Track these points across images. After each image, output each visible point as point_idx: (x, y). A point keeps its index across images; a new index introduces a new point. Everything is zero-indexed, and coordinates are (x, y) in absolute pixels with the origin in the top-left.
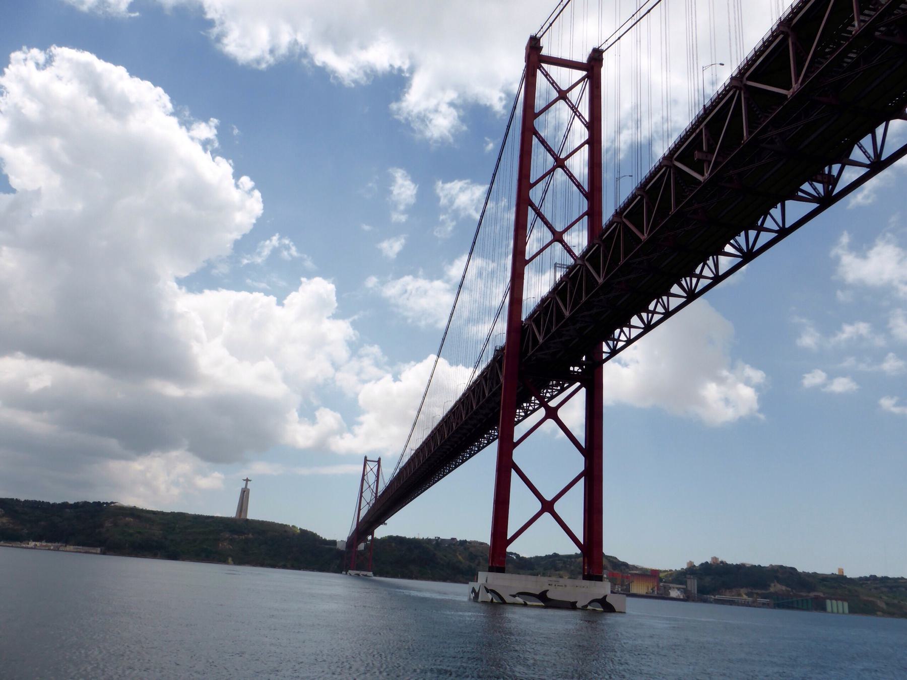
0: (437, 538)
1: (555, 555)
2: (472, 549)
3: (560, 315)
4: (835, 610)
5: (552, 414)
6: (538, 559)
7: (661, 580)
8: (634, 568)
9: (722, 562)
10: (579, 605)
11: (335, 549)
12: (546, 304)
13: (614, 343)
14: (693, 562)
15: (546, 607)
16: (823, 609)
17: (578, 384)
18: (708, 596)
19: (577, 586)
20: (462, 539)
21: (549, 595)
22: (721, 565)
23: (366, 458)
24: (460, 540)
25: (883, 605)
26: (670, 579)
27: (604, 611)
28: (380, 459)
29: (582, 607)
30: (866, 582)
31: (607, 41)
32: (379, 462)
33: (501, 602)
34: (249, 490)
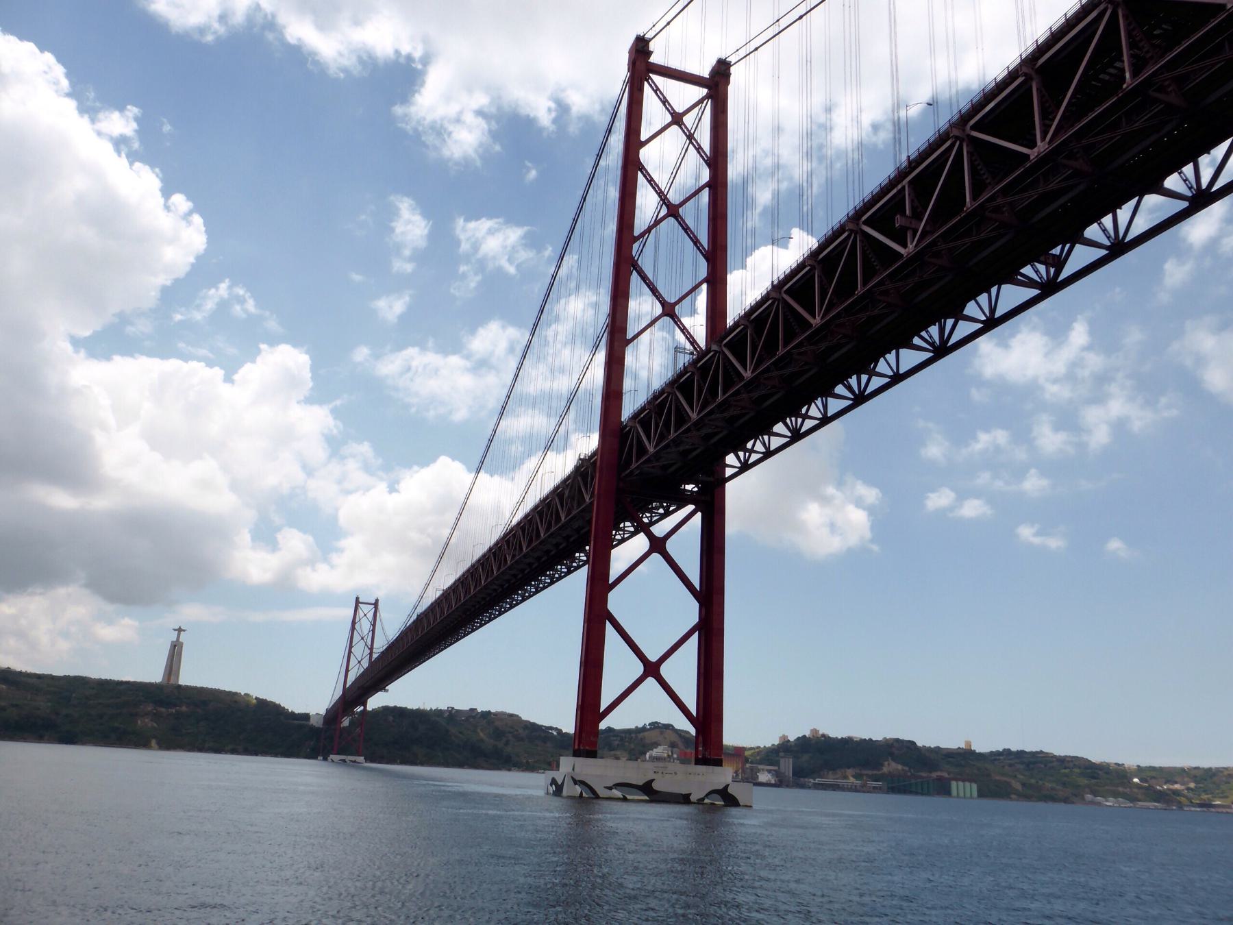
0: (450, 709)
2: (497, 723)
3: (682, 418)
4: (962, 794)
5: (658, 545)
7: (746, 760)
9: (823, 735)
10: (693, 798)
12: (659, 400)
13: (745, 455)
14: (787, 737)
15: (651, 801)
16: (946, 792)
17: (691, 508)
18: (806, 780)
20: (484, 710)
21: (656, 786)
22: (823, 739)
23: (357, 599)
24: (482, 711)
25: (1019, 787)
27: (726, 806)
28: (377, 601)
29: (699, 800)
30: (998, 757)
31: (738, 50)
32: (376, 604)
33: (592, 796)
34: (182, 644)
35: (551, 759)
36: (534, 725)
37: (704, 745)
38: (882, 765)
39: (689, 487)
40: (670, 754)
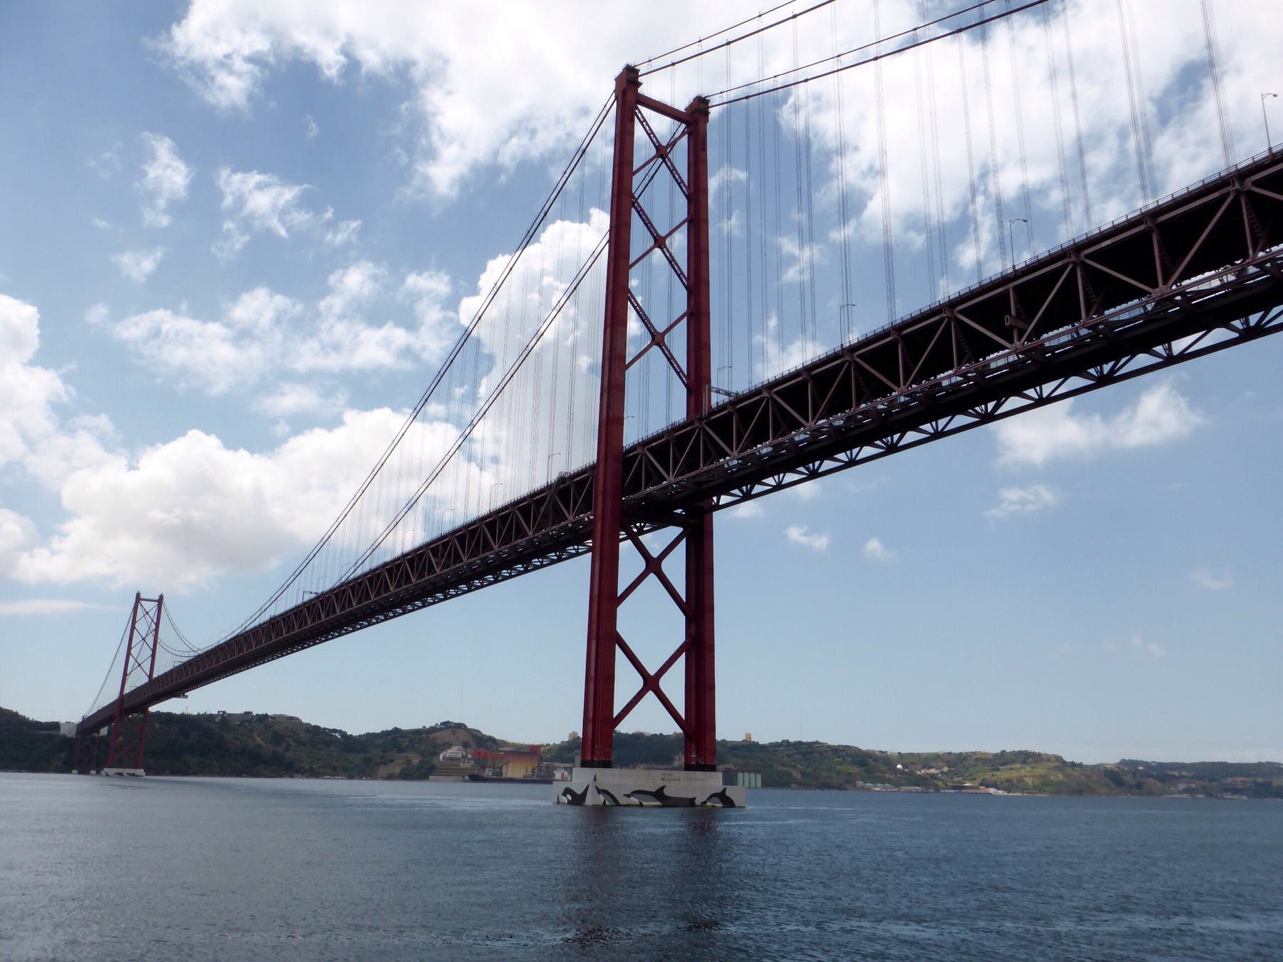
0: (221, 713)
1: (396, 730)
2: (276, 728)
5: (653, 565)
6: (370, 736)
8: (504, 743)
10: (698, 802)
11: (58, 735)
14: (577, 734)
17: (674, 531)
19: (691, 779)
21: (667, 792)
23: (138, 595)
25: (798, 776)
26: (549, 755)
27: (724, 807)
28: (161, 597)
29: (702, 803)
32: (160, 601)
33: (614, 804)
35: (337, 764)
36: (317, 727)
37: (698, 753)
38: (673, 759)
39: (679, 511)
40: (464, 754)
